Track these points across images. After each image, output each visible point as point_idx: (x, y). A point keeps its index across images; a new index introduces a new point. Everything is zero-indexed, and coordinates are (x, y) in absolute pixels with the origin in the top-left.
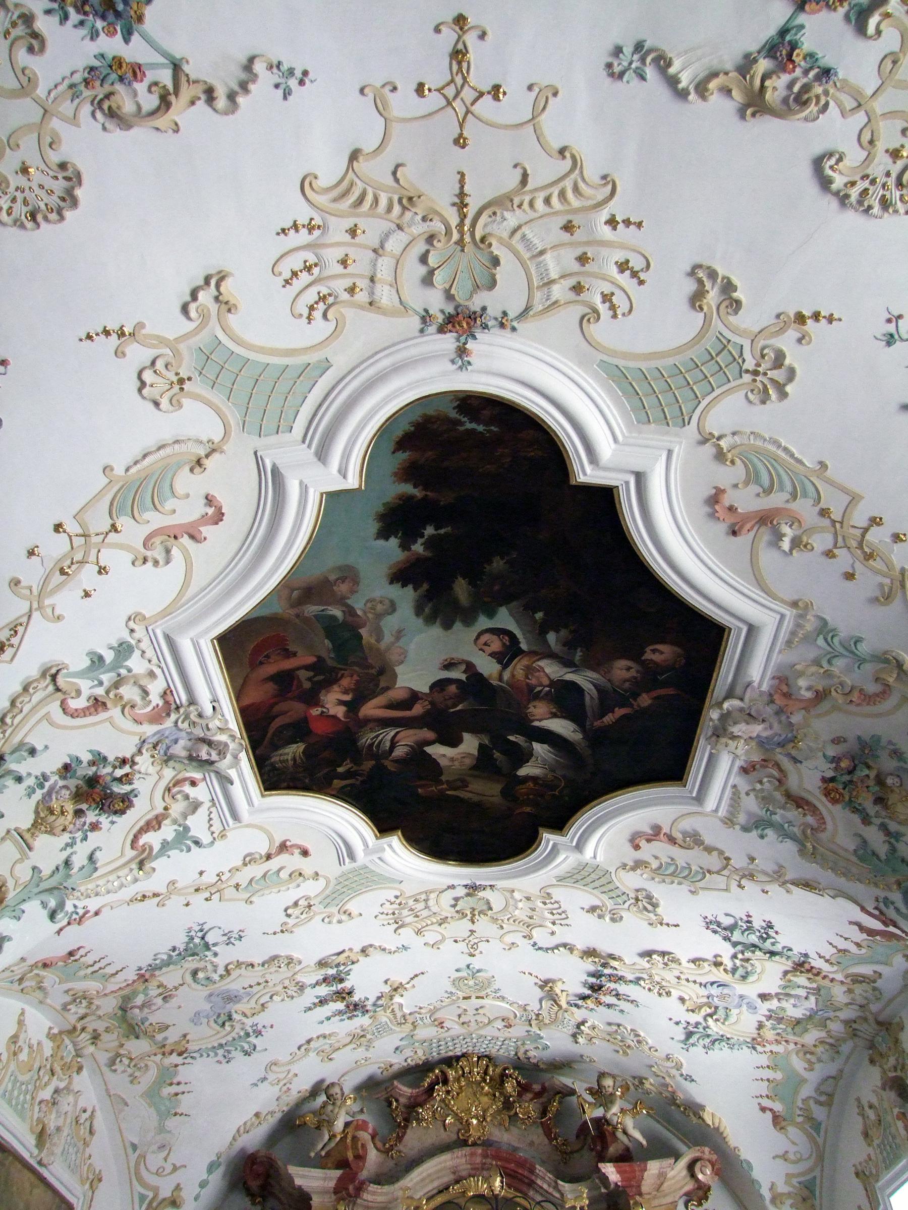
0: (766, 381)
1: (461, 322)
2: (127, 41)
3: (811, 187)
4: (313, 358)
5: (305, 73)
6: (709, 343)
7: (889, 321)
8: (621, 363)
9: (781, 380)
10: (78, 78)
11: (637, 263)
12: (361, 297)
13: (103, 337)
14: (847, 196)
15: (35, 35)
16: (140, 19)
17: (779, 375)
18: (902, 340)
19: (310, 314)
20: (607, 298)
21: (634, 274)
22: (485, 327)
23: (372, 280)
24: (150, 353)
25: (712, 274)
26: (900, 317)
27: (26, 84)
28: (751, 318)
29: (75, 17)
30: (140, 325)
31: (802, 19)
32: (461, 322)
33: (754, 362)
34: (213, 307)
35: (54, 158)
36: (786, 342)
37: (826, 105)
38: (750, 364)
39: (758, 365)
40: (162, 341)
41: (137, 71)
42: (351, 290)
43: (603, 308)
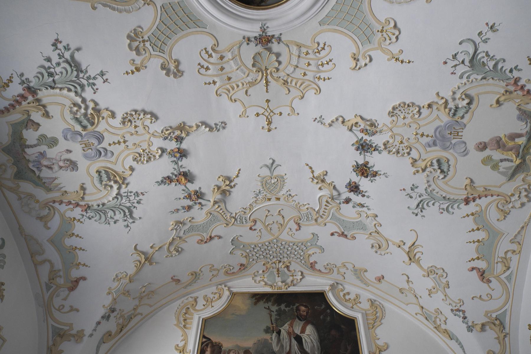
0: (138, 39)
1: (265, 40)
2: (362, 137)
3: (155, 111)
4: (326, 27)
5: (314, 121)
6: (166, 49)
7: (107, 80)
8: (198, 29)
9: (132, 43)
10: (378, 134)
11: (203, 71)
12: (304, 50)
13: (405, 61)
14: (144, 115)
15: (385, 144)
16: (357, 142)
17: (136, 44)
18: (98, 74)
19: (324, 46)
20: (210, 56)
21: (202, 67)
22: (255, 38)
23: (299, 56)
24: (391, 48)
25: (175, 76)
26: (104, 82)
27: (393, 137)
28: (155, 63)
29: (374, 145)
30: (388, 60)
31: (178, 146)
32: (265, 40)
33: (146, 46)
34: (360, 57)
35: (394, 118)
36: (138, 60)
37: (162, 132)
38: (148, 44)
39: (144, 45)
40: (383, 51)
41: (362, 131)
42: (307, 53)
43: (211, 51)
